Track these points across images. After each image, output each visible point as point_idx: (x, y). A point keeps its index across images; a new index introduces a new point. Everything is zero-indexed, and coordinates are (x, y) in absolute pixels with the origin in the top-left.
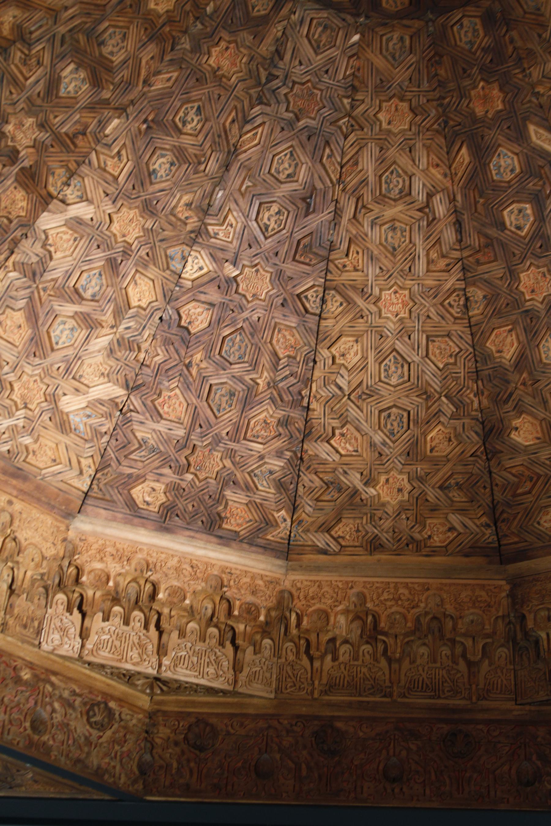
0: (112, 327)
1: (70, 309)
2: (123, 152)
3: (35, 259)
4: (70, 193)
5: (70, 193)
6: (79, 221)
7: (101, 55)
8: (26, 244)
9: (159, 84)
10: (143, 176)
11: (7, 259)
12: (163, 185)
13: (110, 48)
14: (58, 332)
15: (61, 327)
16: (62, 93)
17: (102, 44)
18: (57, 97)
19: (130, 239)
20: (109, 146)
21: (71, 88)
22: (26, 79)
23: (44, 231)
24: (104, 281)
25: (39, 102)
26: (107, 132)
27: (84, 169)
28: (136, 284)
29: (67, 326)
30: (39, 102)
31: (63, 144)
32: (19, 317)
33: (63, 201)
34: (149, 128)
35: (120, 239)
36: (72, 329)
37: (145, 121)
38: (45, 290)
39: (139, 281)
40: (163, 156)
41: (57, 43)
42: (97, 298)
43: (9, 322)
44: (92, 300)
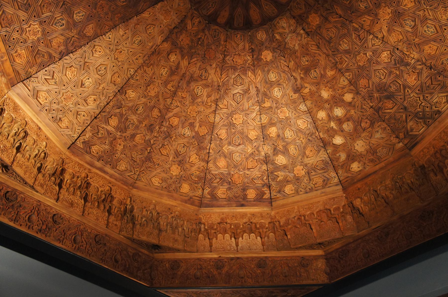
0: (425, 11)
1: (420, 28)
2: (362, 20)
3: (405, 44)
4: (380, 36)
5: (380, 36)
6: (389, 30)
7: (335, 37)
8: (400, 48)
9: (340, 12)
10: (368, 11)
11: (406, 55)
12: (369, 3)
13: (332, 34)
14: (430, 33)
15: (427, 32)
16: (348, 48)
17: (331, 38)
18: (349, 49)
19: (389, 11)
20: (362, 25)
21: (346, 46)
22: (346, 61)
23: (394, 42)
24: (407, 18)
25: (352, 55)
26: (358, 27)
27: (372, 32)
28: (406, 5)
29: (427, 30)
30: (352, 55)
31: (364, 43)
32: (426, 47)
33: (383, 38)
34: (353, 12)
35: (391, 15)
36: (428, 27)
37: (351, 14)
38: (414, 40)
39: (405, 4)
40: (359, 6)
41: (335, 53)
42: (413, 19)
43: (428, 51)
44: (415, 21)
